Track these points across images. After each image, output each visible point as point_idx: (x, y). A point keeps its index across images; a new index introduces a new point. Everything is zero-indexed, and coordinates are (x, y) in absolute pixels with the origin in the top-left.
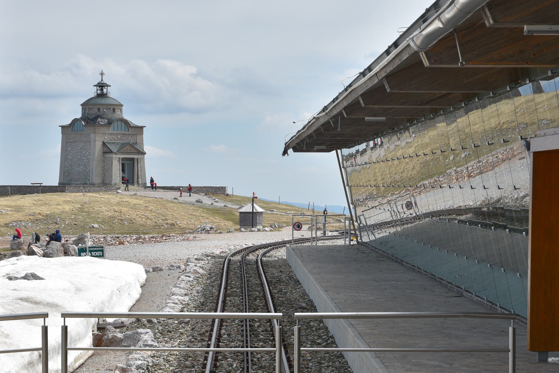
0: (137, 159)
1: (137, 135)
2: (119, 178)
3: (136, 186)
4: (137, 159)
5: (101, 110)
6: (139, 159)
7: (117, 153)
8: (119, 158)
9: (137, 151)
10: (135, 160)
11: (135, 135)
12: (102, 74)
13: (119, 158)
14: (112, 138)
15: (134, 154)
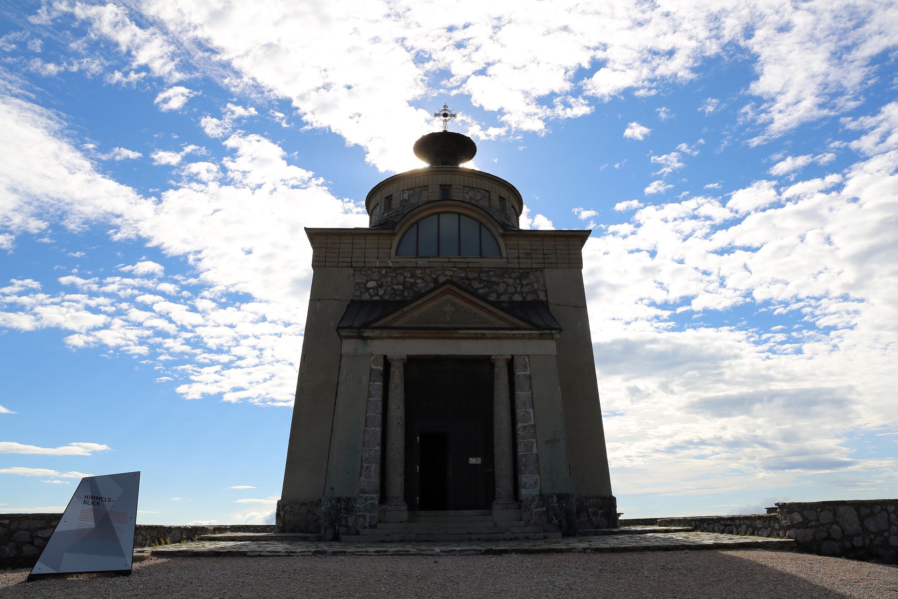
0: (510, 363)
1: (546, 270)
2: (375, 468)
3: (502, 514)
4: (510, 363)
5: (395, 203)
6: (517, 362)
7: (367, 333)
8: (381, 361)
9: (501, 318)
10: (496, 370)
11: (538, 274)
12: (445, 115)
13: (387, 363)
14: (405, 288)
15: (483, 337)
